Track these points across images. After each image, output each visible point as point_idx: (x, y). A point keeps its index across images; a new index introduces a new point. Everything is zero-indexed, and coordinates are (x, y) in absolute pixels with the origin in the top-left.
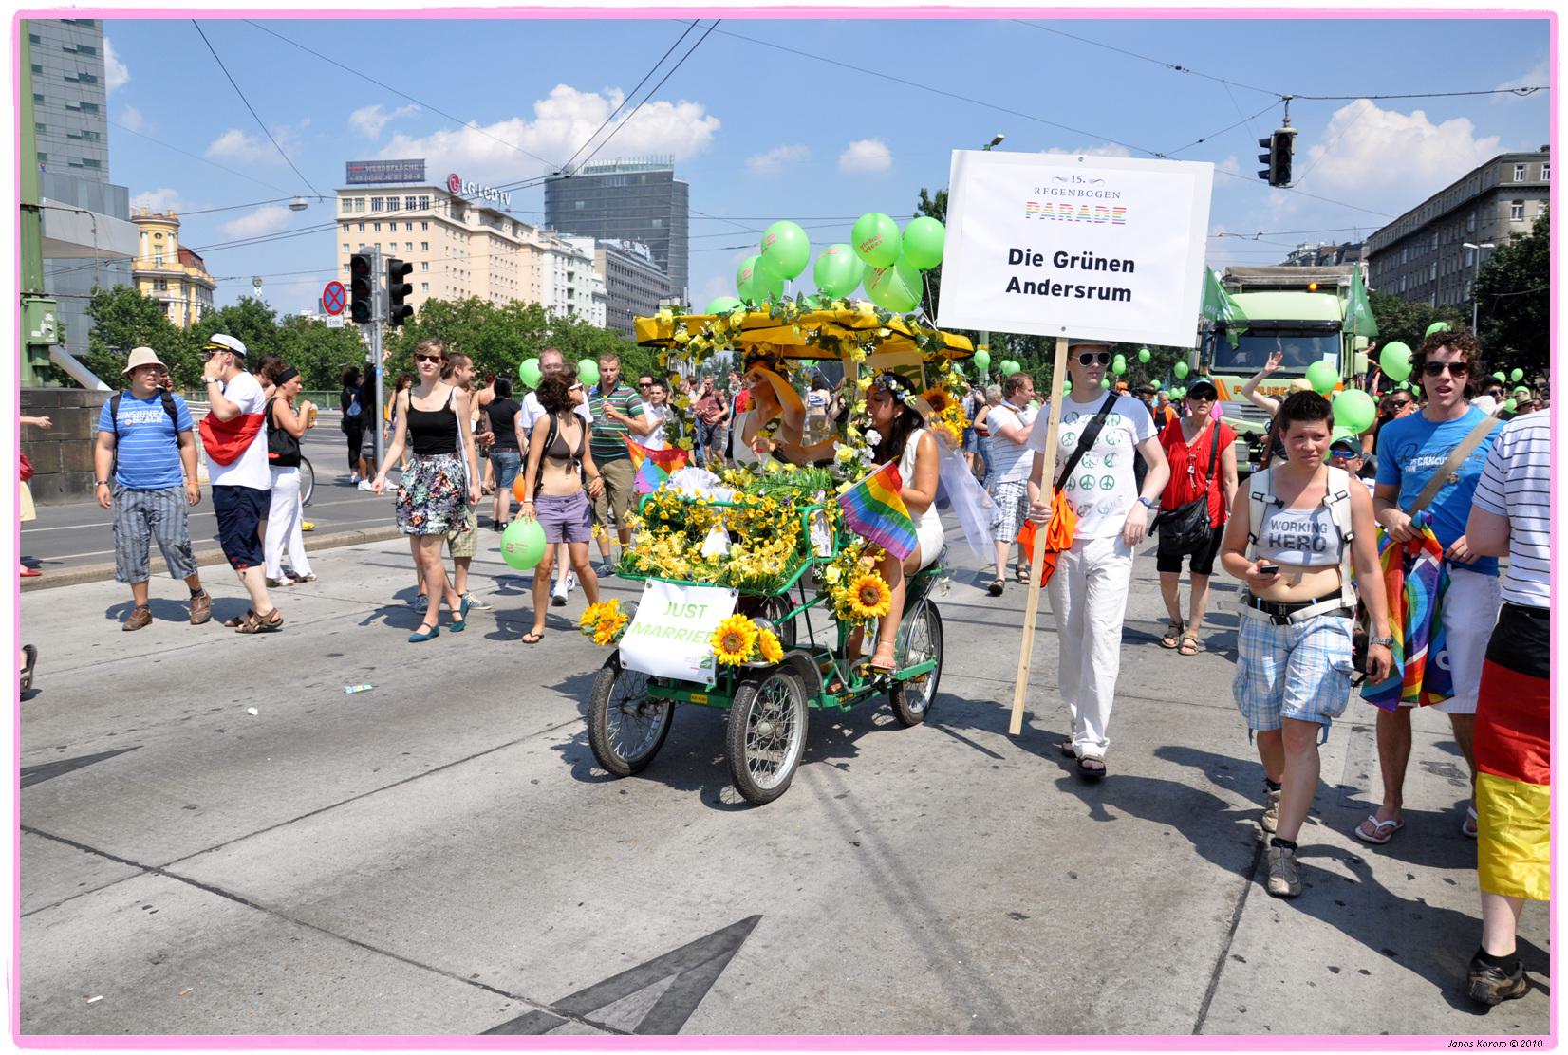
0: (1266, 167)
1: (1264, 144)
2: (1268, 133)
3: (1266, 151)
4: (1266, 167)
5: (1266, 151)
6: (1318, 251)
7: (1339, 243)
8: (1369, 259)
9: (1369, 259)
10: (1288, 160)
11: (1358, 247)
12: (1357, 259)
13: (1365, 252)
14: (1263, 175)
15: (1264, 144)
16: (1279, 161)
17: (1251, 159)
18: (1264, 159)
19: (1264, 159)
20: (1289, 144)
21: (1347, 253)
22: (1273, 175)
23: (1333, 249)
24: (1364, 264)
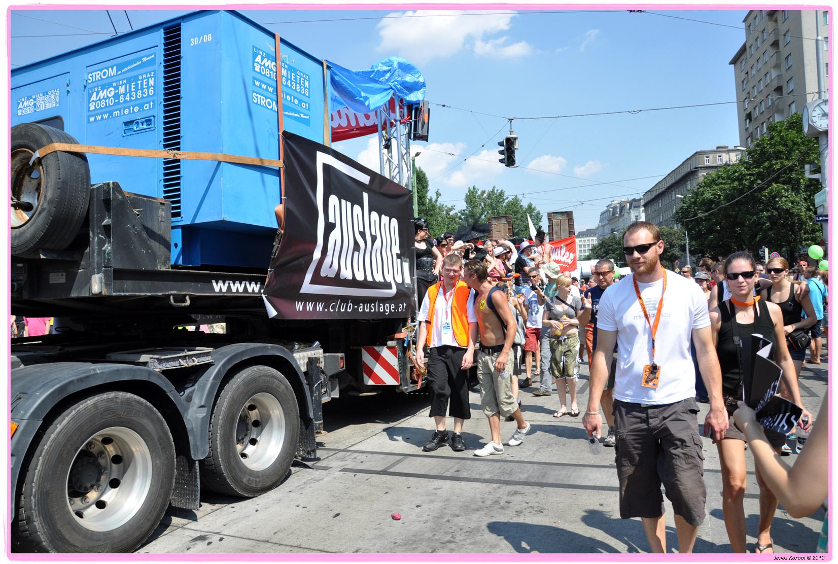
0: (503, 157)
1: (501, 144)
2: (502, 139)
3: (502, 148)
4: (503, 157)
5: (502, 148)
6: (620, 204)
7: (631, 199)
8: (645, 206)
9: (645, 206)
10: (513, 152)
11: (640, 200)
12: (639, 207)
13: (642, 202)
14: (501, 161)
15: (501, 144)
17: (495, 155)
19: (501, 152)
21: (634, 204)
23: (627, 202)
24: (642, 209)
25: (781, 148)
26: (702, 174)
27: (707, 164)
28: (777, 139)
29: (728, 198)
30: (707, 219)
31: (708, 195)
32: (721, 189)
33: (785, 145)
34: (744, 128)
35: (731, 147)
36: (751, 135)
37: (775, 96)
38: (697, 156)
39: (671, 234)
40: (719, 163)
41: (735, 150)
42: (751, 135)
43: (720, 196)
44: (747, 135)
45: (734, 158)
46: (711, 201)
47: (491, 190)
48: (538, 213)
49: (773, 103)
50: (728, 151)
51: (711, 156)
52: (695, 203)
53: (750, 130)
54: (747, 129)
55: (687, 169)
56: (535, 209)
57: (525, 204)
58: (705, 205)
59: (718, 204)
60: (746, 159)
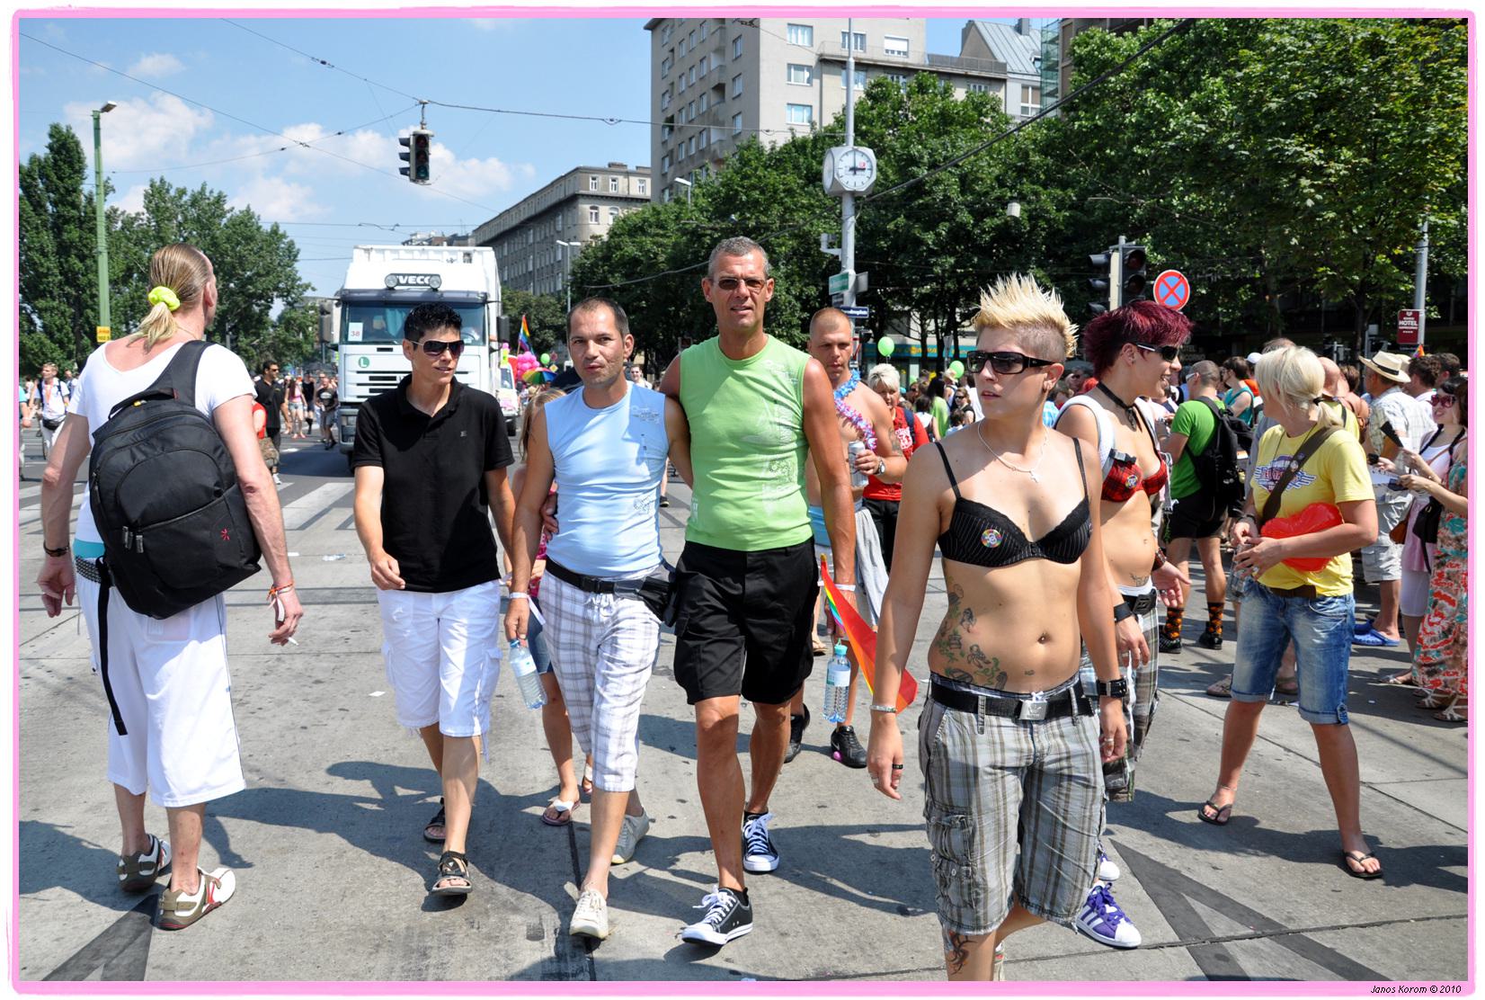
0: (406, 164)
1: (405, 142)
2: (406, 134)
3: (406, 150)
4: (406, 164)
5: (406, 150)
10: (426, 159)
14: (404, 171)
15: (405, 142)
16: (418, 158)
18: (404, 157)
19: (404, 157)
20: (426, 144)
22: (413, 172)
25: (756, 194)
26: (585, 207)
27: (592, 190)
28: (754, 180)
29: (674, 261)
30: (622, 289)
31: (630, 249)
32: (661, 245)
33: (762, 192)
34: (659, 141)
35: (631, 168)
36: (671, 154)
37: (714, 98)
38: (578, 175)
39: (539, 305)
40: (612, 192)
41: (640, 172)
42: (671, 154)
43: (656, 254)
44: (668, 157)
45: (639, 187)
46: (635, 261)
47: (198, 189)
48: (291, 244)
49: (709, 108)
50: (628, 174)
51: (600, 178)
52: (607, 258)
53: (671, 146)
54: (664, 143)
55: (559, 195)
56: (284, 236)
57: (266, 228)
58: (624, 265)
59: (652, 265)
60: (703, 202)
